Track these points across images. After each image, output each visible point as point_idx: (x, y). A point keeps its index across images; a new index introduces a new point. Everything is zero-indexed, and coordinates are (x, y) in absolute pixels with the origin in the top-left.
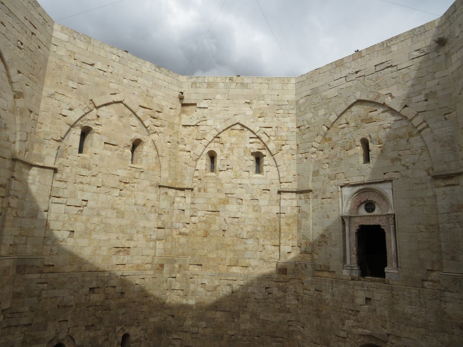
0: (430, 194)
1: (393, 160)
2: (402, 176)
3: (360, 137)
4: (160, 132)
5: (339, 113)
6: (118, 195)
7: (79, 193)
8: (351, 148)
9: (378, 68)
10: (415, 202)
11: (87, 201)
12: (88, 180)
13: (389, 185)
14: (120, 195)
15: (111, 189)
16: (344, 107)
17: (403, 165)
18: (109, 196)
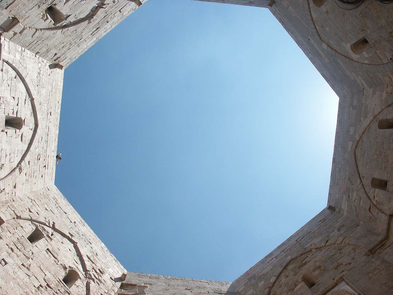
0: (378, 263)
1: (336, 268)
2: (349, 270)
3: (301, 276)
4: (97, 282)
5: (277, 274)
6: (37, 286)
7: (5, 253)
8: (296, 286)
9: (298, 240)
10: (371, 275)
11: (6, 263)
12: (19, 253)
13: (343, 283)
14: (38, 288)
15: (33, 276)
16: (280, 269)
17: (346, 265)
18: (28, 280)
